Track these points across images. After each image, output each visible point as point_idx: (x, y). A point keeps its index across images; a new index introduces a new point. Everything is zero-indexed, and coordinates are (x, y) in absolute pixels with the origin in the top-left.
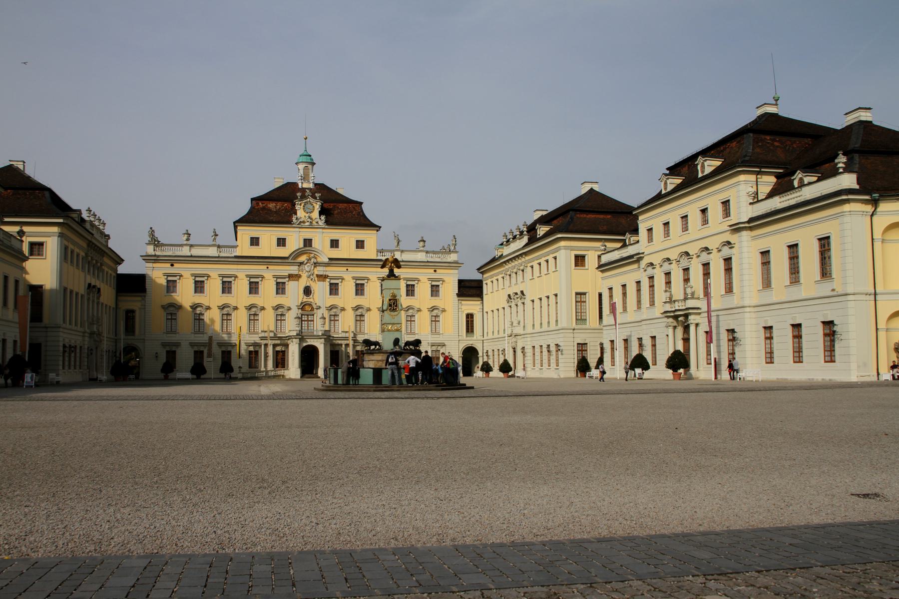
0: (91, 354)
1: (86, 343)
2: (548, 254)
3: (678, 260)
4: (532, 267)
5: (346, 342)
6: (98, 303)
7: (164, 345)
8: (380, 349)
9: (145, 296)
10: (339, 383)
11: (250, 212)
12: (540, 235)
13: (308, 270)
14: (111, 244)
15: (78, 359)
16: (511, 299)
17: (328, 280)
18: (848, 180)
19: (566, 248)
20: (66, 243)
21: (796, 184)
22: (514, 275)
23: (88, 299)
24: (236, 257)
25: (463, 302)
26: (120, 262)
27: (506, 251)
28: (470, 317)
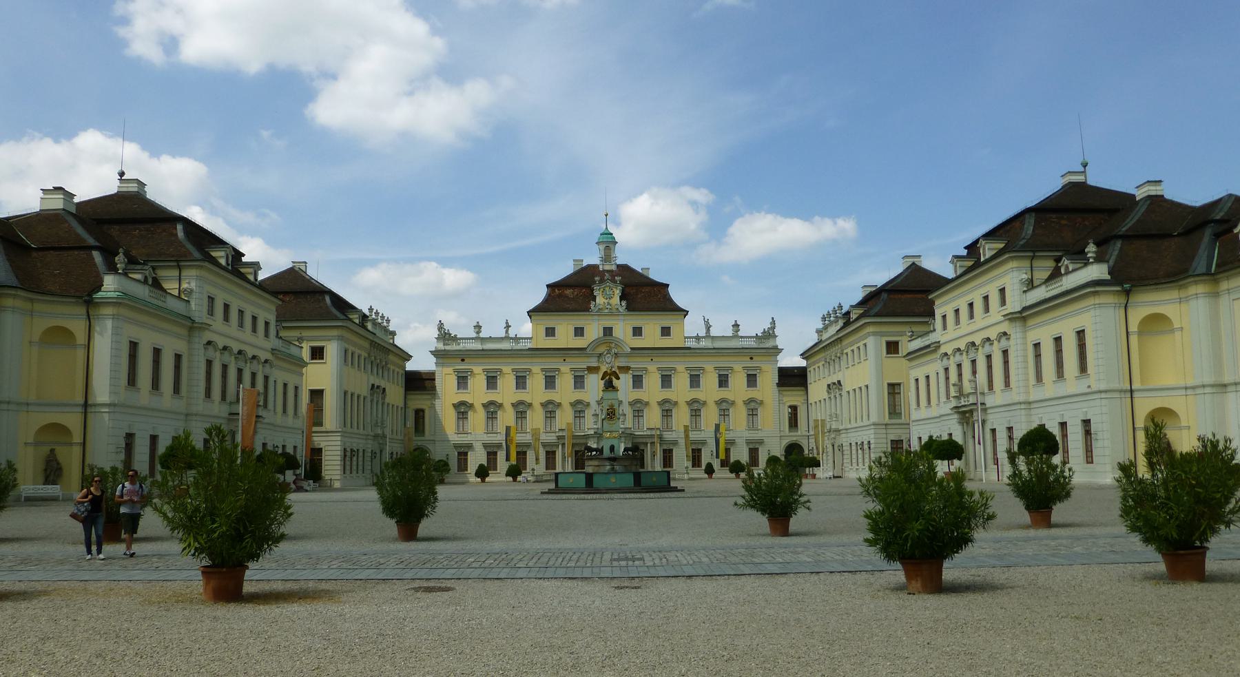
0: (375, 457)
1: (370, 446)
5: (651, 440)
6: (383, 404)
7: (456, 446)
9: (435, 394)
11: (546, 301)
13: (608, 361)
14: (399, 341)
15: (360, 463)
16: (830, 389)
17: (631, 372)
18: (1097, 271)
19: (875, 334)
20: (347, 346)
21: (1063, 271)
22: (832, 363)
23: (372, 401)
24: (530, 349)
25: (785, 393)
26: (407, 358)
27: (825, 336)
28: (794, 409)
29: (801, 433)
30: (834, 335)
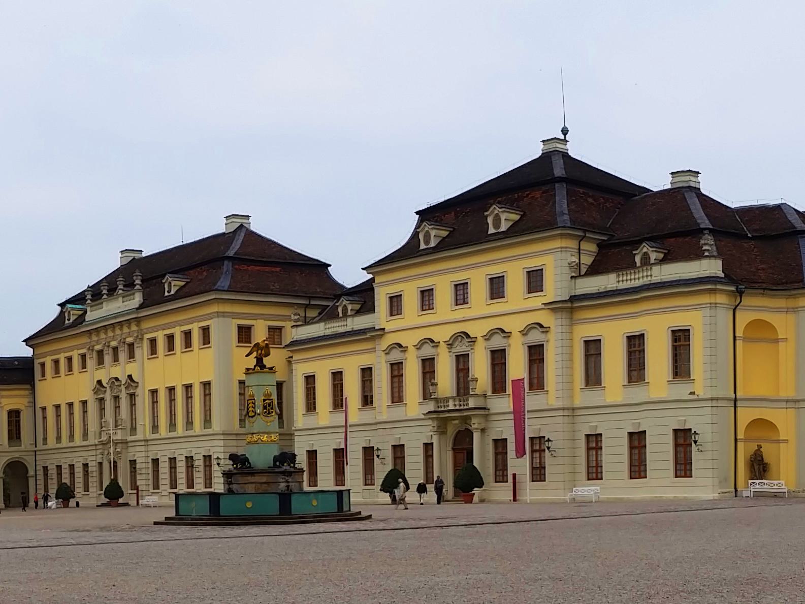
2: (191, 321)
3: (450, 343)
4: (153, 342)
8: (250, 467)
10: (221, 514)
12: (172, 292)
29: (26, 448)
30: (129, 312)
